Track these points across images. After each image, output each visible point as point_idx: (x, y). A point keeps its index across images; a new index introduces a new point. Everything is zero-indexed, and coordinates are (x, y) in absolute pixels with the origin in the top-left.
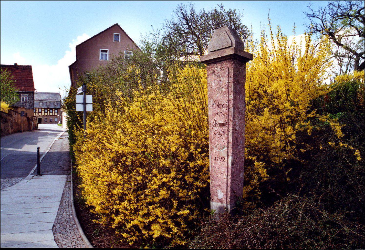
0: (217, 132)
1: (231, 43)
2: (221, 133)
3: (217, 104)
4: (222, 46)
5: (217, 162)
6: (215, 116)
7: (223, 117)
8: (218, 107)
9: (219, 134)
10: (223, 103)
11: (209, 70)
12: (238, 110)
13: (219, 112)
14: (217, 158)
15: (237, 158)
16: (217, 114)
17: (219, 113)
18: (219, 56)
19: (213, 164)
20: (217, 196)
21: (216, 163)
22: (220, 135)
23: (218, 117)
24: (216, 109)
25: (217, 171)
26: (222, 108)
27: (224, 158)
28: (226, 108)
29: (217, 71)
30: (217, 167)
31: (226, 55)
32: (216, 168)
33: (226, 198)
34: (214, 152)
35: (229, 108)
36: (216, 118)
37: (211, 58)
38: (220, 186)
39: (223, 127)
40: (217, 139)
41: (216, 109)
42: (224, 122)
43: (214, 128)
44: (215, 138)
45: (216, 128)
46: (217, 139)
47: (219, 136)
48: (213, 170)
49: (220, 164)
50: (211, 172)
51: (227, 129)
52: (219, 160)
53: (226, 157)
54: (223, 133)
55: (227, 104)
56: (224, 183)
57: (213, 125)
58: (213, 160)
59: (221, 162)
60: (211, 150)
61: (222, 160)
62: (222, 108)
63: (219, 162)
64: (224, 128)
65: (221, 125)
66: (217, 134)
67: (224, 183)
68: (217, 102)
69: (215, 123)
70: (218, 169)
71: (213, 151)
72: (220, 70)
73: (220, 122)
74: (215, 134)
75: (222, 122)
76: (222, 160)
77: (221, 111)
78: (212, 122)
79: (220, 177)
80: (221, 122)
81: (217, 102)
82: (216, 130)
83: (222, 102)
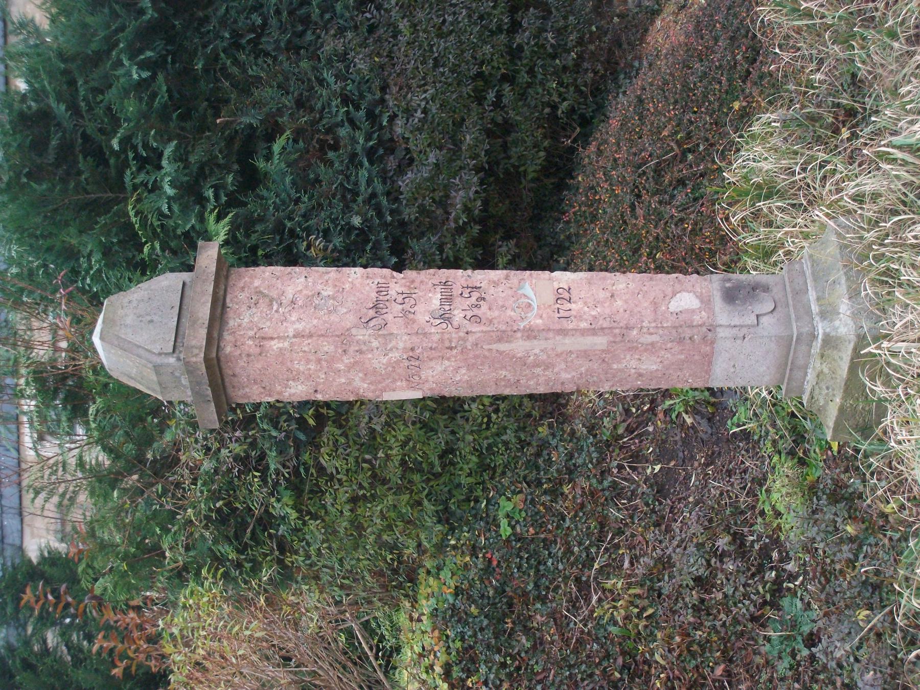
0: (469, 314)
2: (474, 299)
3: (372, 313)
5: (573, 313)
6: (414, 321)
7: (420, 294)
8: (385, 311)
10: (374, 295)
13: (400, 307)
14: (562, 314)
16: (405, 313)
17: (407, 306)
19: (584, 325)
20: (693, 311)
21: (579, 317)
22: (482, 303)
23: (420, 308)
24: (389, 317)
25: (607, 311)
26: (388, 297)
28: (392, 285)
30: (594, 313)
31: (213, 268)
32: (595, 317)
34: (539, 321)
36: (422, 317)
38: (655, 305)
41: (389, 317)
43: (455, 324)
44: (491, 321)
45: (458, 316)
47: (484, 306)
48: (606, 324)
49: (580, 305)
52: (568, 306)
54: (475, 295)
56: (645, 289)
57: (444, 326)
61: (566, 295)
62: (388, 297)
63: (573, 306)
64: (457, 291)
65: (448, 299)
66: (476, 311)
68: (366, 314)
76: (566, 295)
77: (400, 300)
78: (433, 330)
79: (626, 302)
80: (435, 300)
82: (462, 315)
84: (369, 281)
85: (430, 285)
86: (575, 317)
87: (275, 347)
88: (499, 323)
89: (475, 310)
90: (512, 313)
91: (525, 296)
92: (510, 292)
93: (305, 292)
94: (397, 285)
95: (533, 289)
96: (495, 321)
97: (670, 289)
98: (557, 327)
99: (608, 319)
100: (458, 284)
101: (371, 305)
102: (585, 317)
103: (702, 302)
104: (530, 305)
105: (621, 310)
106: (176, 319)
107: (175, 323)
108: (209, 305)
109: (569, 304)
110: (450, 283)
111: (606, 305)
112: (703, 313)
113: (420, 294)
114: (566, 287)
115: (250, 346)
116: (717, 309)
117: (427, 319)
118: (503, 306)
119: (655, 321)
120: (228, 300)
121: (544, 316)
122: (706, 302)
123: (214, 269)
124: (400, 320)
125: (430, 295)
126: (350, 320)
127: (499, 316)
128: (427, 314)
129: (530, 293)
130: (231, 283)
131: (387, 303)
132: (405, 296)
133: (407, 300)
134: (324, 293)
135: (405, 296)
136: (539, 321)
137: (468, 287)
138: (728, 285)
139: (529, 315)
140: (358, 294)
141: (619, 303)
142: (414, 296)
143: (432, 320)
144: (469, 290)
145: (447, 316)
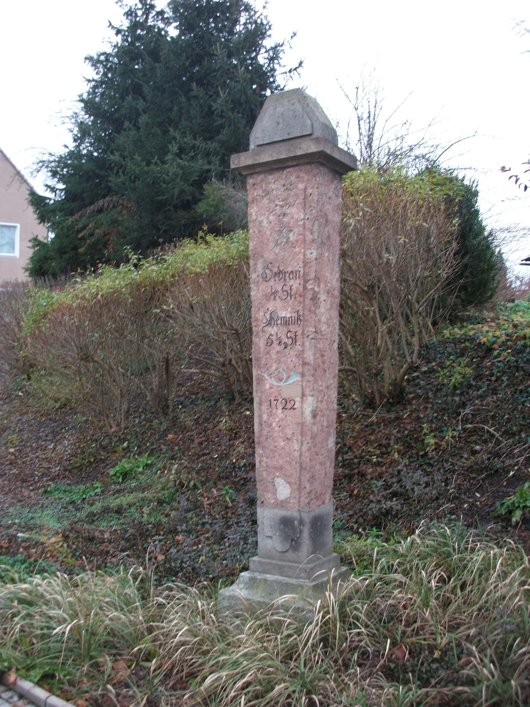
0: (274, 338)
1: (310, 126)
2: (286, 340)
3: (275, 270)
4: (289, 134)
5: (274, 411)
6: (268, 300)
7: (291, 302)
8: (277, 279)
9: (280, 343)
10: (290, 269)
11: (255, 189)
12: (327, 286)
15: (322, 402)
17: (280, 293)
18: (283, 156)
19: (265, 417)
21: (270, 415)
22: (283, 346)
23: (278, 303)
25: (275, 434)
26: (288, 280)
27: (292, 402)
28: (298, 281)
29: (275, 192)
31: (299, 153)
32: (271, 425)
33: (298, 496)
34: (268, 386)
35: (306, 281)
37: (261, 161)
39: (291, 327)
40: (274, 356)
41: (272, 283)
42: (293, 315)
43: (266, 329)
44: (268, 353)
45: (272, 330)
46: (274, 356)
47: (279, 348)
48: (265, 432)
50: (259, 438)
51: (301, 332)
52: (280, 407)
53: (298, 399)
54: (289, 342)
55: (302, 270)
56: (294, 463)
58: (264, 408)
59: (286, 412)
60: (258, 383)
63: (280, 411)
64: (292, 328)
65: (286, 322)
66: (276, 343)
67: (294, 463)
69: (268, 316)
70: (277, 428)
71: (264, 385)
72: (282, 189)
73: (283, 315)
74: (269, 343)
75: (289, 315)
76: (289, 406)
77: (286, 288)
78: (261, 314)
79: (283, 448)
81: (274, 266)
82: (273, 332)
83: (289, 265)
84: (301, 264)
85: (298, 309)
86: (271, 412)
87: (252, 210)
88: (267, 359)
89: (277, 342)
90: (274, 368)
91: (288, 377)
92: (291, 366)
93: (292, 221)
94: (298, 285)
95: (294, 382)
96: (268, 356)
97: (293, 481)
98: (263, 399)
99: (269, 434)
100: (299, 329)
101: (281, 269)
102: (271, 419)
103: (282, 501)
104: (281, 380)
105: (276, 444)
106: (280, 139)
107: (276, 140)
108: (270, 159)
109: (281, 408)
110: (299, 322)
111: (280, 434)
112: (273, 501)
113: (291, 302)
114: (295, 406)
115: (253, 194)
116: (276, 511)
117: (270, 309)
118: (280, 362)
119: (267, 466)
120: (289, 170)
121: (272, 390)
122: (283, 504)
123: (299, 154)
124: (269, 290)
125: (289, 309)
126: (269, 256)
127: (271, 359)
128: (274, 309)
129: (290, 381)
130: (303, 168)
131: (283, 280)
132: (289, 292)
133: (285, 293)
134: (291, 235)
135: (289, 292)
136: (268, 386)
137: (296, 336)
138: (296, 523)
139: (273, 379)
140: (291, 258)
141: (282, 444)
142: (289, 298)
143: (269, 312)
144: (294, 337)
145: (273, 323)
